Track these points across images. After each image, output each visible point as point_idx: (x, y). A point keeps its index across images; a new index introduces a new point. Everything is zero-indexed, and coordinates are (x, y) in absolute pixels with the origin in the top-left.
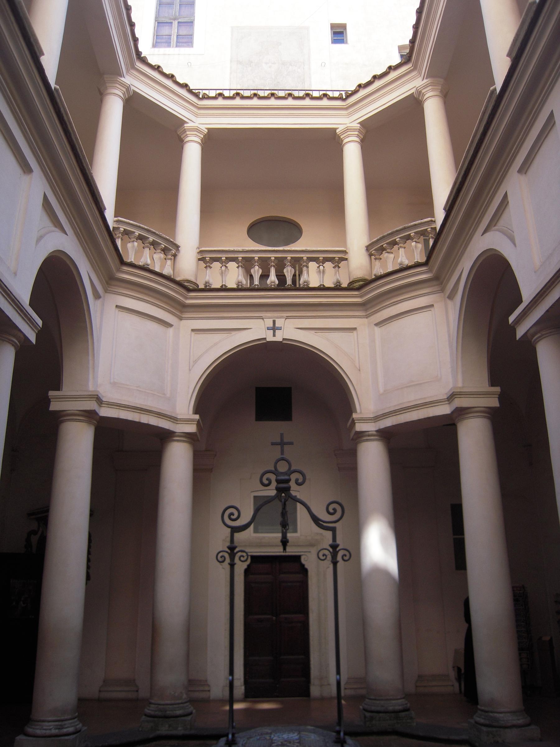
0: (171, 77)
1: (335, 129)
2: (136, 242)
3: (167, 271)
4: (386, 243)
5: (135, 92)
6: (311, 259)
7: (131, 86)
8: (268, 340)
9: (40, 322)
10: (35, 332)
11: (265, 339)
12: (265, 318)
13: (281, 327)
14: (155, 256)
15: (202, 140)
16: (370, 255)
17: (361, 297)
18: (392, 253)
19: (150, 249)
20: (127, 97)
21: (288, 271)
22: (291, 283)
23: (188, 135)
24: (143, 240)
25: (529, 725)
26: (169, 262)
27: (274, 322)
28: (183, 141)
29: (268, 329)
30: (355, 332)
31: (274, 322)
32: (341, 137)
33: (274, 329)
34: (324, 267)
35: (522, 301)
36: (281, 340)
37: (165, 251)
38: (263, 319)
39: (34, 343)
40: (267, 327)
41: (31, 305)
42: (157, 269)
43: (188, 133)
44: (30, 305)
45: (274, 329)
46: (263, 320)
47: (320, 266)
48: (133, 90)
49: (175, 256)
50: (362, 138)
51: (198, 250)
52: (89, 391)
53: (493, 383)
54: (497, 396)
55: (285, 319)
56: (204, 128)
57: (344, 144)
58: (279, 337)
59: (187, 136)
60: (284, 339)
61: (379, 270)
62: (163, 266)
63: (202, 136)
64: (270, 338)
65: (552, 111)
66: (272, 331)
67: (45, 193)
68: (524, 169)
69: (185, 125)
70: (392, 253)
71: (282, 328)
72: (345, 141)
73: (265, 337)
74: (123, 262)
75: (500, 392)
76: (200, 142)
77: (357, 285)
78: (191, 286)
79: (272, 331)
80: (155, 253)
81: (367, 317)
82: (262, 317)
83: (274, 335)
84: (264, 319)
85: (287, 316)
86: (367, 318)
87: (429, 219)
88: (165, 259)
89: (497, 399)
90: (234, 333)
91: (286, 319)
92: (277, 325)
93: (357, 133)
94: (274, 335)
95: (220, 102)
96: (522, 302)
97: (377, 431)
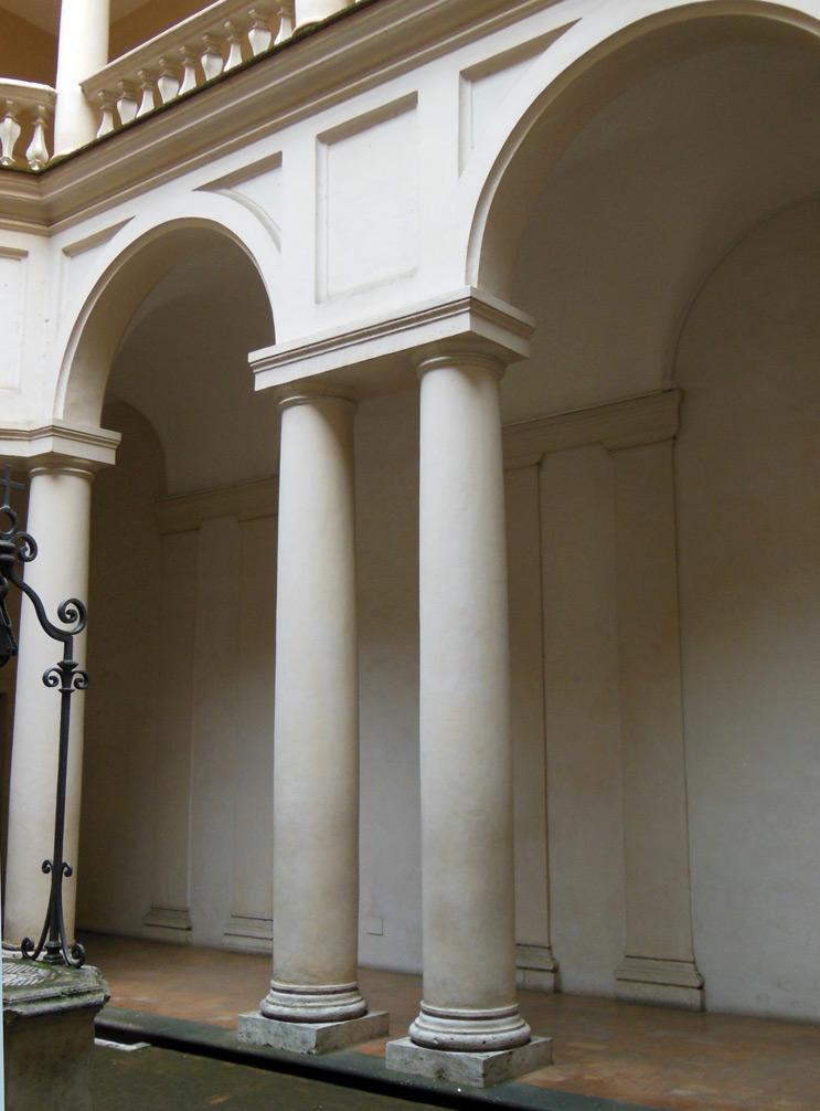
87: (47, 87)
89: (114, 452)
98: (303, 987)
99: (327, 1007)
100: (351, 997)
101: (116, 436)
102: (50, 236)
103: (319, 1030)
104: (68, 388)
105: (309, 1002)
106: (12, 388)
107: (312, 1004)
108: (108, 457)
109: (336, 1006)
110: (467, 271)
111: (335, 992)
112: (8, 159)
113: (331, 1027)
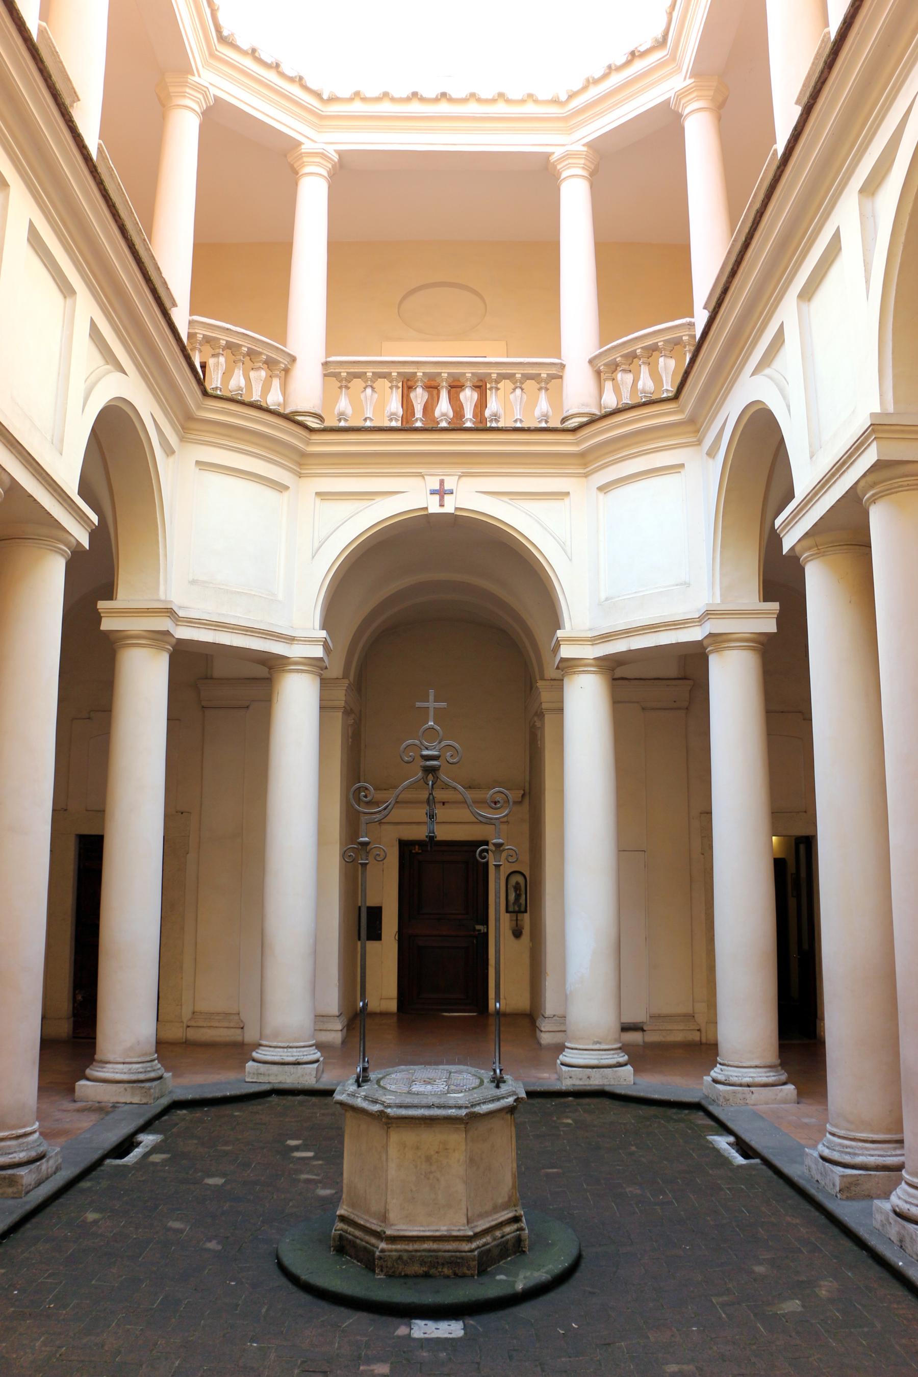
0: (276, 67)
1: (549, 155)
2: (223, 355)
3: (274, 399)
4: (621, 356)
5: (217, 99)
6: (502, 377)
7: (211, 88)
8: (431, 511)
9: (95, 518)
10: (87, 530)
11: (426, 508)
12: (427, 475)
13: (453, 490)
14: (252, 374)
15: (329, 173)
16: (598, 373)
17: (577, 444)
18: (630, 371)
19: (243, 364)
20: (205, 108)
21: (466, 397)
22: (471, 417)
23: (306, 164)
24: (233, 349)
25: (785, 1084)
26: (276, 383)
27: (442, 482)
28: (297, 173)
29: (431, 494)
30: (567, 500)
31: (442, 482)
32: (559, 167)
33: (441, 493)
34: (522, 390)
35: (794, 497)
36: (452, 510)
37: (270, 364)
38: (423, 476)
39: (88, 548)
40: (430, 490)
41: (81, 493)
42: (256, 397)
43: (305, 159)
44: (79, 494)
45: (441, 493)
46: (424, 478)
47: (516, 387)
48: (214, 95)
49: (287, 371)
50: (593, 168)
51: (323, 360)
52: (158, 600)
53: (768, 594)
54: (776, 616)
55: (457, 477)
56: (331, 151)
57: (563, 179)
58: (449, 508)
59: (303, 165)
60: (456, 509)
61: (610, 401)
62: (266, 389)
63: (330, 166)
64: (434, 508)
65: (838, 228)
66: (437, 497)
67: (92, 319)
68: (807, 294)
69: (303, 147)
70: (630, 371)
71: (454, 492)
72: (564, 175)
73: (426, 506)
74: (205, 393)
75: (780, 610)
76: (325, 174)
77: (573, 423)
78: (312, 423)
79: (437, 497)
80: (252, 369)
81: (586, 475)
82: (421, 473)
83: (442, 505)
84: (425, 477)
85: (462, 473)
86: (586, 477)
88: (271, 376)
89: (775, 620)
90: (378, 499)
91: (460, 477)
92: (447, 487)
93: (582, 161)
94: (442, 505)
95: (357, 107)
96: (794, 497)
97: (594, 659)
98: (842, 1133)
99: (862, 1155)
100: (895, 1149)
101: (775, 606)
102: (699, 444)
103: (843, 1176)
104: (721, 574)
105: (847, 1147)
106: (685, 583)
107: (848, 1150)
108: (770, 626)
109: (872, 1156)
110: (881, 395)
111: (873, 1142)
112: (667, 390)
113: (860, 1175)
